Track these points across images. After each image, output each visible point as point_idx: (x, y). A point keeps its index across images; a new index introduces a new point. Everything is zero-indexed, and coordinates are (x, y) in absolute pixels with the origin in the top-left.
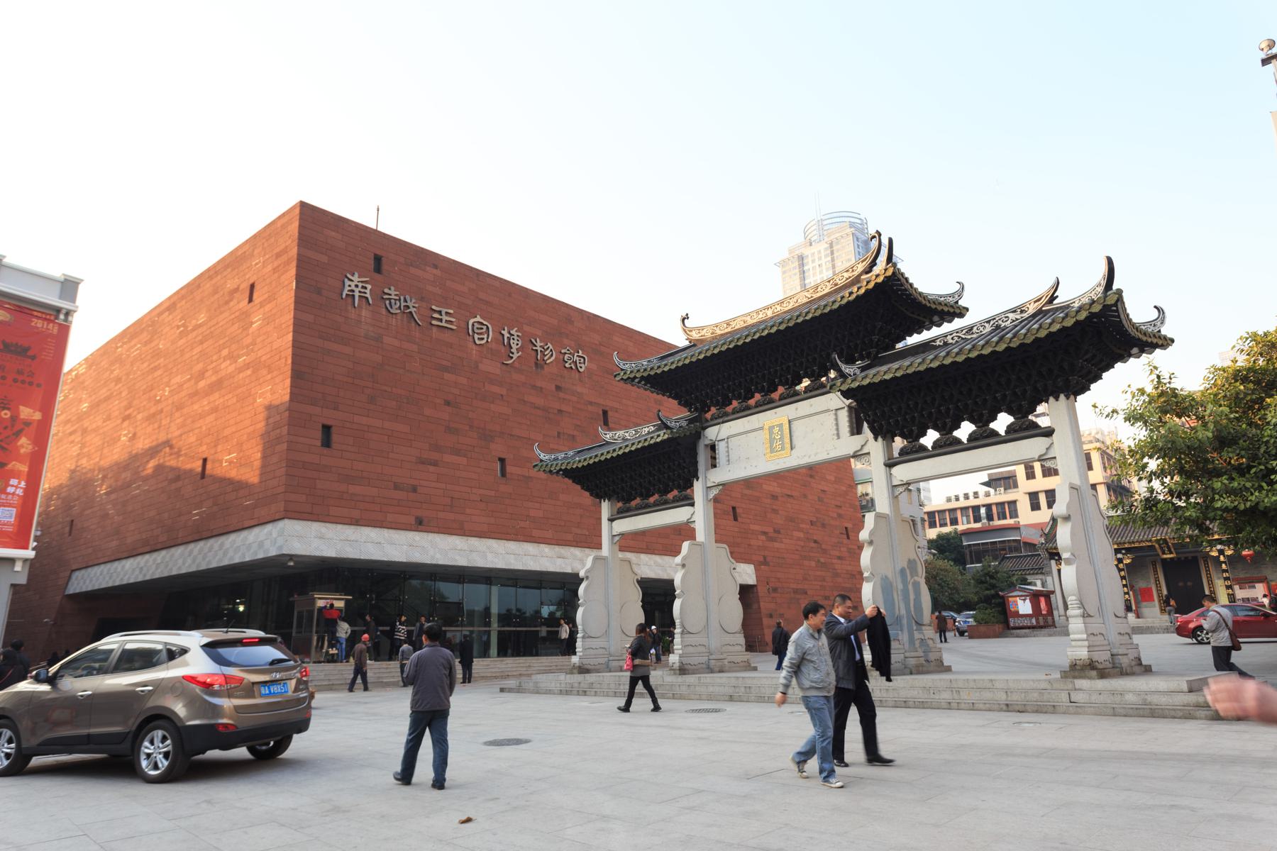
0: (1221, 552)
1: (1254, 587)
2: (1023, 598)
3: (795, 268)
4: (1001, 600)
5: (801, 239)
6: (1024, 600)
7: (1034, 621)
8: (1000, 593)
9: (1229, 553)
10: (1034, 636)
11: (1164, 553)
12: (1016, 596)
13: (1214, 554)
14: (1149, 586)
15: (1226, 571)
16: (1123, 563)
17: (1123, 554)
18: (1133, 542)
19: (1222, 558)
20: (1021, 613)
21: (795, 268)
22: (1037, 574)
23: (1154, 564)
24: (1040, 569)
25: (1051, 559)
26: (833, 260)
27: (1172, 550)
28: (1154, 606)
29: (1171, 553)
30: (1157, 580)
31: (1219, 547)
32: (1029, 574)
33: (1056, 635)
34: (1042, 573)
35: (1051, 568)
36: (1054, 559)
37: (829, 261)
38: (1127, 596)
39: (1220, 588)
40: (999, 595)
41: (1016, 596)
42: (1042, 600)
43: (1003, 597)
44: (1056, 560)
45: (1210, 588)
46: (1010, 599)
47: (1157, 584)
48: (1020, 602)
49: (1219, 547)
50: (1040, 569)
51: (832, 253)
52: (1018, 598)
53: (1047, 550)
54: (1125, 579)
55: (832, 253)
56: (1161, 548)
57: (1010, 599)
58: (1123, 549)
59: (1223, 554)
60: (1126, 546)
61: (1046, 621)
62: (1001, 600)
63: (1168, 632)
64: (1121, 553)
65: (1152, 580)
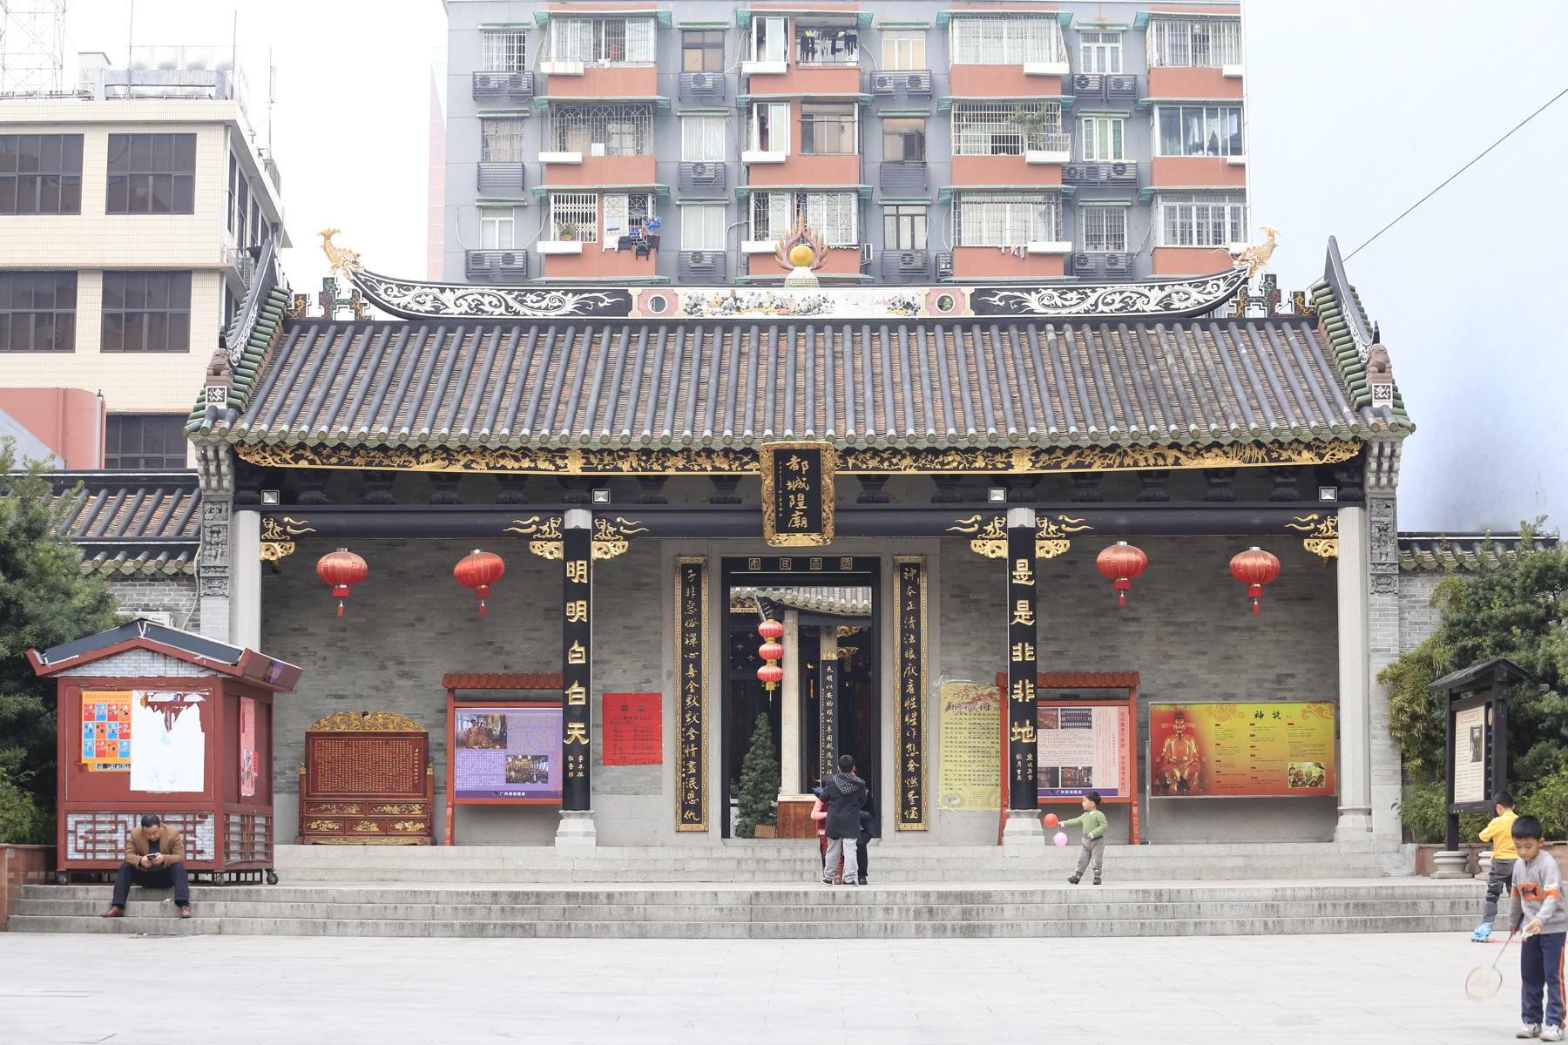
0: (1022, 542)
1: (1085, 721)
2: (167, 697)
4: (33, 703)
6: (172, 709)
7: (205, 838)
8: (37, 654)
9: (1050, 549)
10: (220, 930)
11: (783, 526)
12: (126, 684)
13: (993, 548)
14: (647, 689)
15: (1023, 634)
16: (587, 556)
17: (598, 512)
18: (666, 452)
19: (1022, 569)
20: (135, 785)
22: (154, 578)
23: (691, 576)
24: (173, 552)
25: (240, 503)
27: (828, 509)
28: (655, 787)
29: (815, 526)
30: (691, 657)
31: (1021, 517)
32: (118, 577)
33: (341, 930)
34: (179, 577)
35: (233, 552)
36: (253, 504)
38: (576, 730)
39: (947, 717)
40: (26, 664)
41: (126, 684)
42: (249, 709)
43: (48, 688)
44: (266, 513)
45: (904, 712)
46: (88, 697)
47: (685, 680)
48: (144, 720)
49: (1021, 517)
50: (173, 552)
52: (136, 696)
53: (232, 451)
54: (585, 643)
56: (782, 494)
57: (88, 697)
58: (600, 483)
59: (1029, 553)
60: (626, 468)
61: (247, 847)
62: (33, 703)
63: (939, 932)
64: (586, 503)
65: (671, 659)
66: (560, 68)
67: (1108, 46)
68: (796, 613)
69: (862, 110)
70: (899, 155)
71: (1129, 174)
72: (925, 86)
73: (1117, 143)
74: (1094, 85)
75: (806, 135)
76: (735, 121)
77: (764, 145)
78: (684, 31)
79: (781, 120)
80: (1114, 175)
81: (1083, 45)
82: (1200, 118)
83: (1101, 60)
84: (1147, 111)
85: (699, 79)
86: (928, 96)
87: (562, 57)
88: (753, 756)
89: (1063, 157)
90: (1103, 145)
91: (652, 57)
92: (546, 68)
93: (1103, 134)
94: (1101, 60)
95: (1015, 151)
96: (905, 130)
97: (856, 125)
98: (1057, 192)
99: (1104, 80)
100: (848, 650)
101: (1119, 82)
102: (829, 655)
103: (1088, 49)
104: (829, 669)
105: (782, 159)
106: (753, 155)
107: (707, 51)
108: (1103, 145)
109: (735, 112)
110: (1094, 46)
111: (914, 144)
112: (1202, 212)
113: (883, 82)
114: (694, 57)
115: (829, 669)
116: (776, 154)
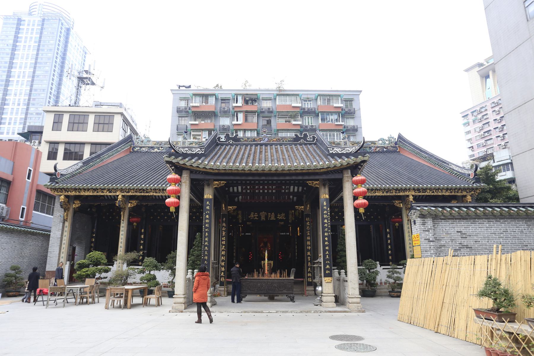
3: (14, 24)
5: (27, 10)
21: (14, 24)
26: (42, 29)
37: (39, 29)
51: (43, 25)
55: (43, 25)
66: (194, 105)
67: (309, 103)
68: (188, 172)
69: (258, 115)
70: (266, 124)
71: (314, 127)
72: (271, 110)
73: (311, 121)
74: (306, 110)
75: (246, 120)
76: (231, 117)
77: (237, 121)
78: (222, 100)
79: (241, 116)
80: (311, 128)
81: (304, 103)
82: (329, 116)
83: (308, 105)
84: (318, 116)
85: (224, 108)
86: (272, 112)
87: (195, 103)
88: (193, 250)
89: (300, 123)
90: (309, 122)
91: (214, 103)
92: (191, 105)
93: (308, 120)
94: (308, 105)
95: (290, 122)
96: (267, 119)
97: (256, 117)
98: (299, 130)
99: (308, 109)
100: (233, 207)
101: (312, 109)
102: (208, 195)
103: (305, 103)
104: (208, 203)
105: (241, 123)
106: (235, 122)
107: (226, 104)
108: (309, 122)
109: (231, 115)
110: (306, 103)
111: (269, 122)
112: (330, 135)
113: (262, 109)
114: (223, 105)
115: (208, 203)
116: (239, 122)
